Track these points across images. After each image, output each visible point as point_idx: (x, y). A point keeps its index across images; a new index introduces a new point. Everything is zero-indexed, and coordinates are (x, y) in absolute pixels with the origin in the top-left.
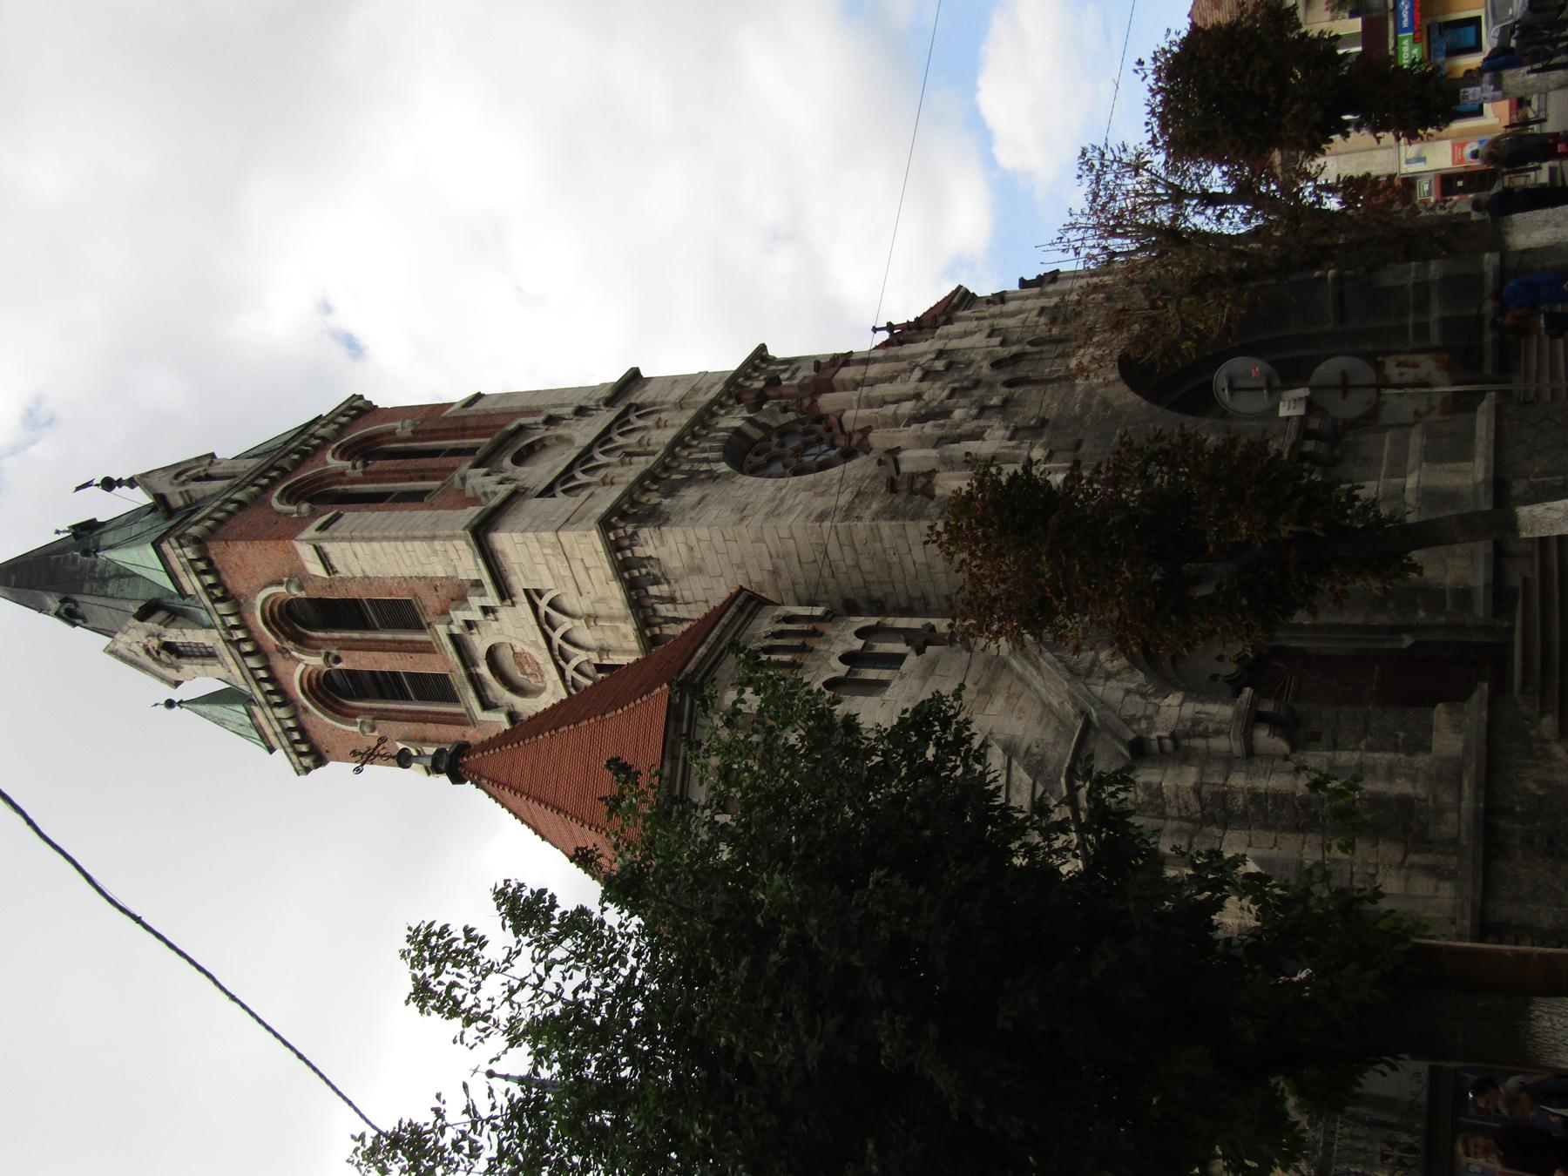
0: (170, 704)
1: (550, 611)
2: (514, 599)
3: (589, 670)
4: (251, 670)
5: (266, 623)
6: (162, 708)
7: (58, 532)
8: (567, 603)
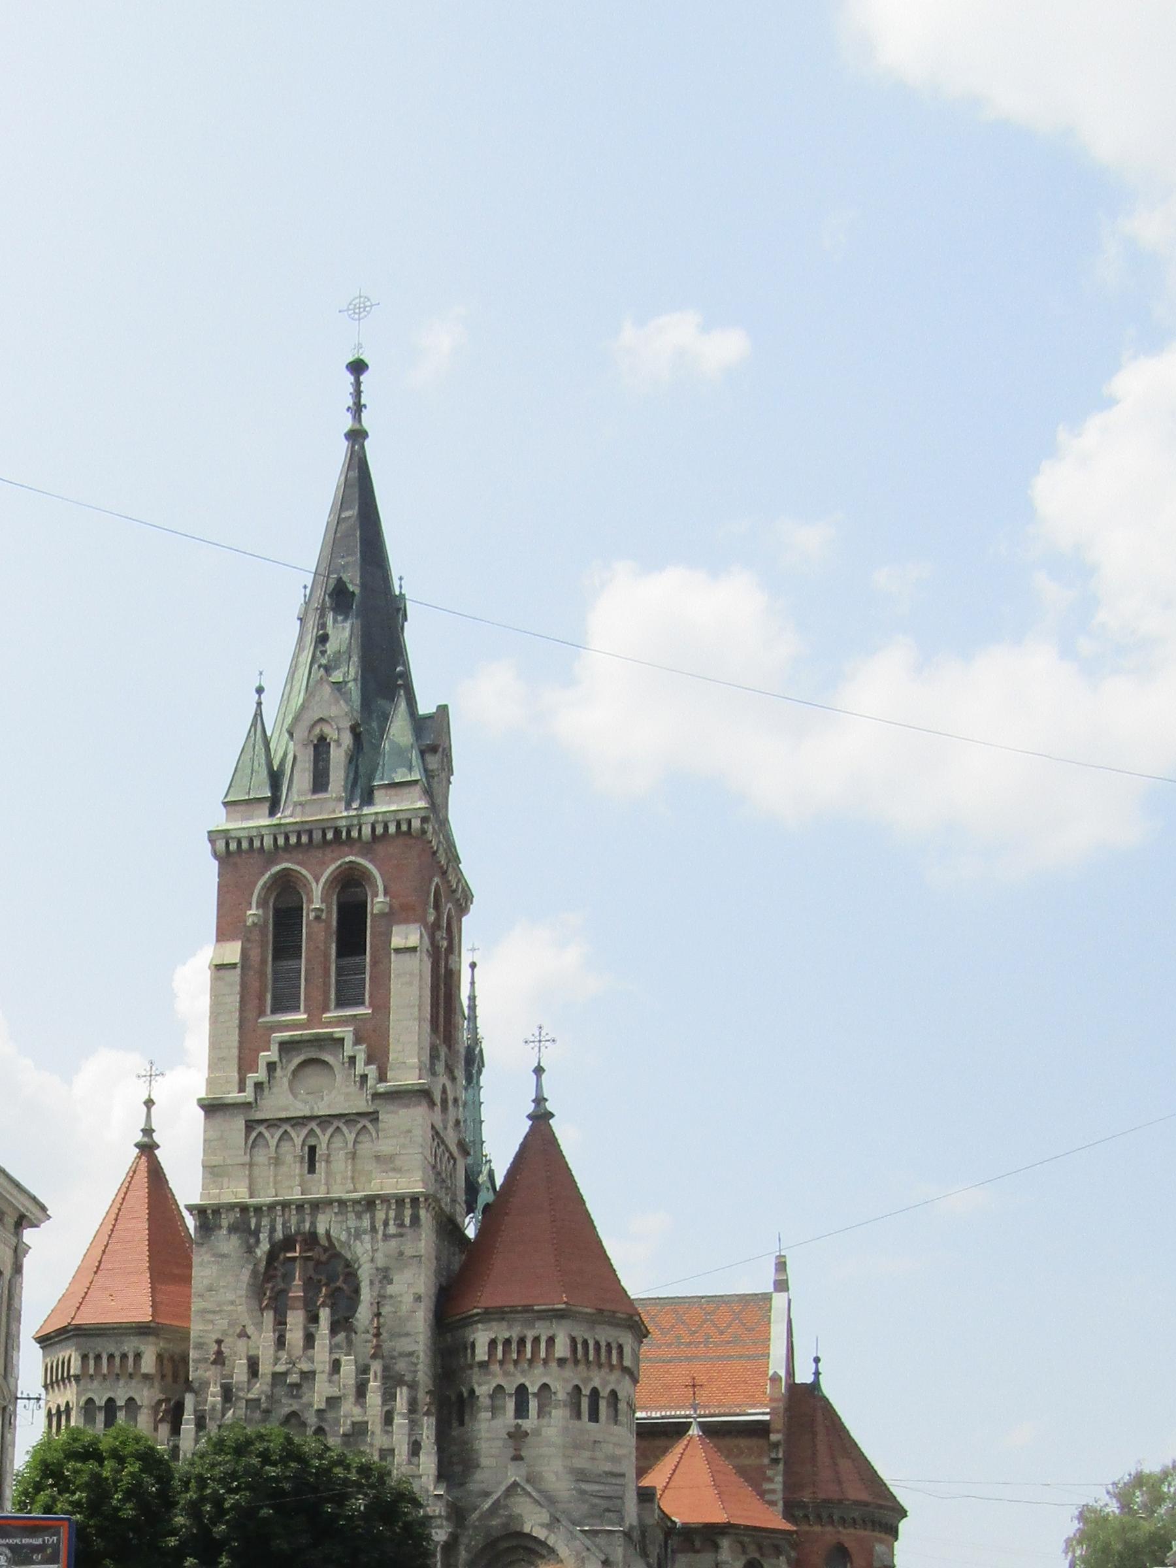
0: (260, 690)
1: (359, 1126)
2: (370, 1103)
3: (312, 1141)
4: (310, 833)
5: (350, 862)
6: (257, 684)
7: (401, 579)
8: (361, 1138)
